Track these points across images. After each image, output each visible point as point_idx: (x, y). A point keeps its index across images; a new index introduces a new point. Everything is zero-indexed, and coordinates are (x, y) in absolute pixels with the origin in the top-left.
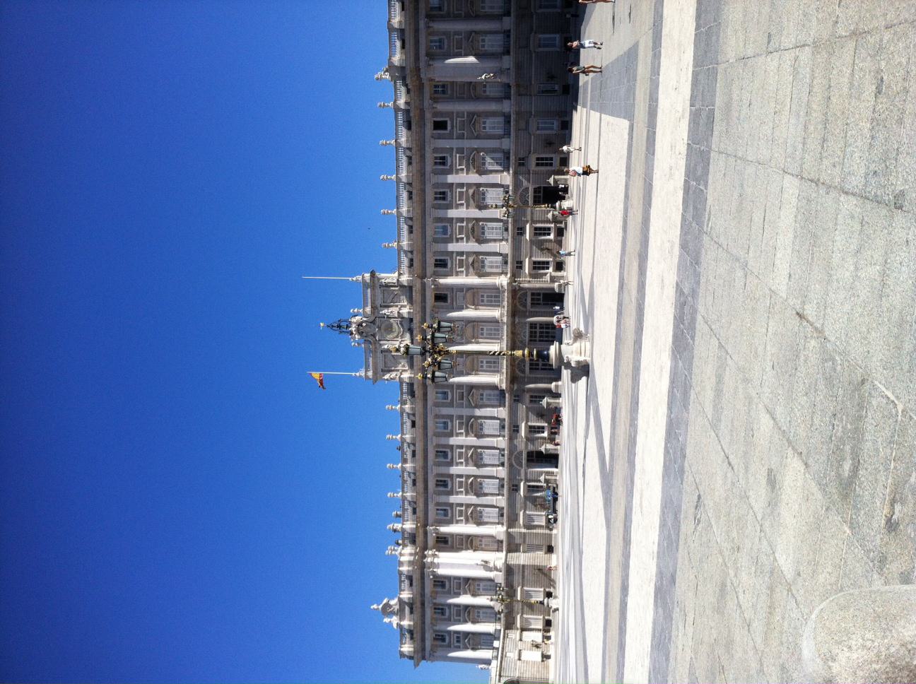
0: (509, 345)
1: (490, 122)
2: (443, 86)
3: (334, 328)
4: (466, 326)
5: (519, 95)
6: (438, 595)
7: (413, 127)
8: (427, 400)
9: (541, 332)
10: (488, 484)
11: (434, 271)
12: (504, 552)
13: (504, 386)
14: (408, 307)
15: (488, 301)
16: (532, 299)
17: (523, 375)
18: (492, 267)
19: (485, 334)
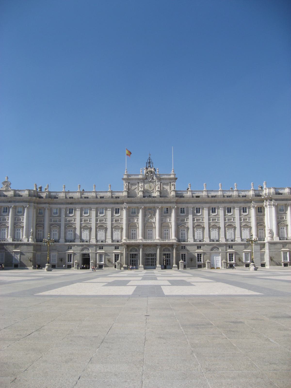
0: (147, 244)
2: (261, 212)
3: (149, 160)
5: (260, 245)
6: (14, 209)
8: (115, 204)
9: (149, 259)
10: (71, 234)
11: (179, 208)
13: (123, 241)
14: (161, 195)
15: (165, 233)
16: (168, 254)
17: (129, 250)
18: (182, 234)
19: (149, 232)
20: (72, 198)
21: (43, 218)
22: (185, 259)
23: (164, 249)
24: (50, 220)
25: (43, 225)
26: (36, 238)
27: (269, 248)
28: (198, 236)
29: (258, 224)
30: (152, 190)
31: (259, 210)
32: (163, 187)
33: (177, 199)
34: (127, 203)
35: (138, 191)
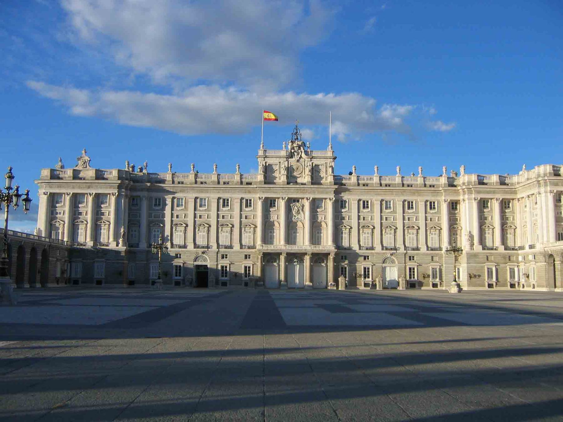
1: (436, 237)
4: (301, 221)
7: (432, 189)
12: (129, 248)
14: (313, 181)
17: (266, 260)
20: (182, 183)
21: (138, 211)
22: (345, 274)
23: (316, 259)
24: (150, 215)
25: (139, 222)
26: (128, 241)
27: (467, 261)
28: (365, 242)
29: (452, 227)
30: (300, 174)
31: (453, 206)
32: (315, 170)
33: (336, 188)
34: (263, 192)
35: (280, 175)
